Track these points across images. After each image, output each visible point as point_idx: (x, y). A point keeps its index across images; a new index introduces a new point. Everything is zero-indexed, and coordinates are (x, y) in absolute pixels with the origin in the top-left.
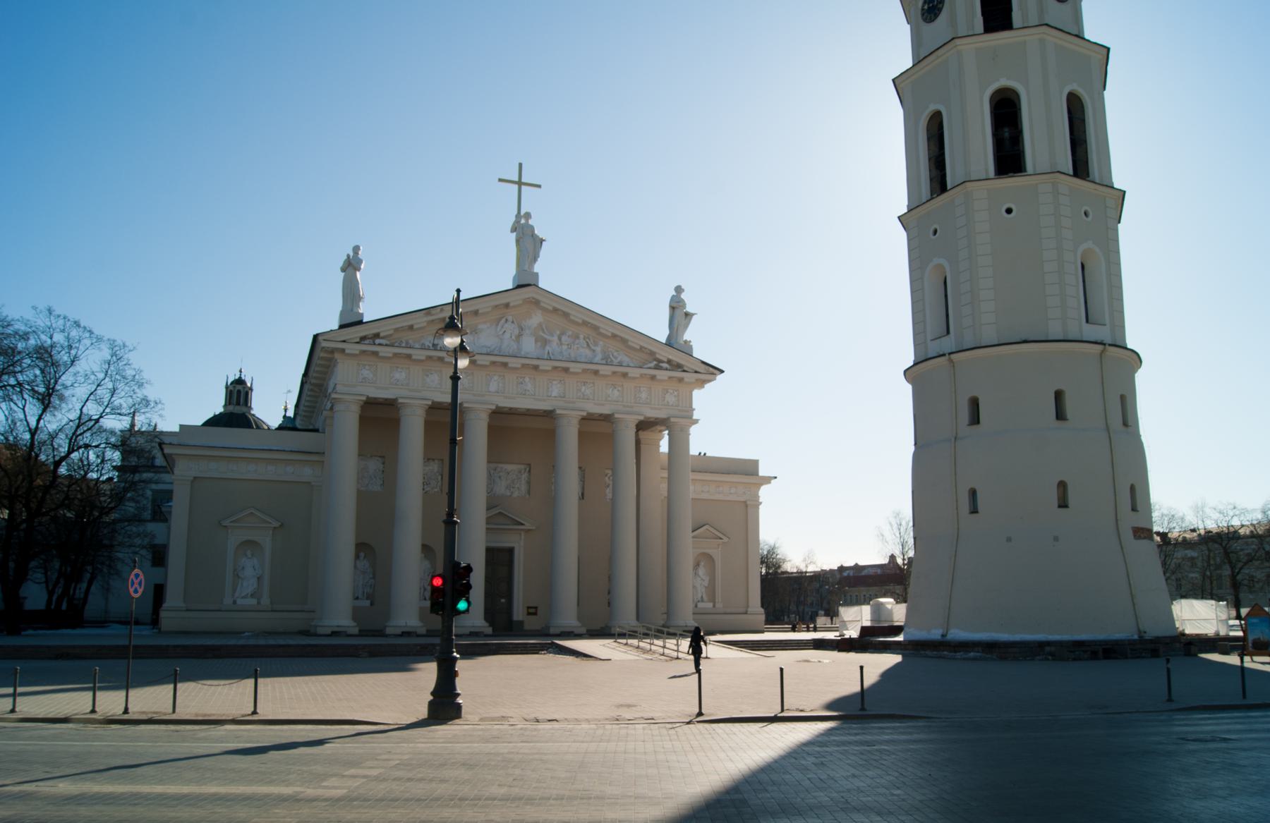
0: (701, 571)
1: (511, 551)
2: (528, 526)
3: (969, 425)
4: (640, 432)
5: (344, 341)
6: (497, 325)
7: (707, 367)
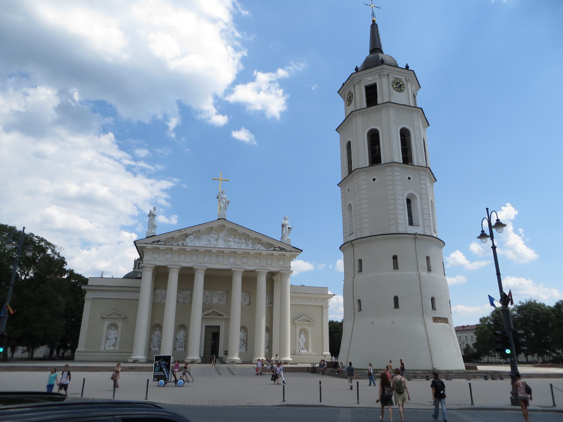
0: (302, 336)
2: (225, 317)
3: (358, 272)
4: (274, 277)
5: (146, 243)
7: (295, 249)
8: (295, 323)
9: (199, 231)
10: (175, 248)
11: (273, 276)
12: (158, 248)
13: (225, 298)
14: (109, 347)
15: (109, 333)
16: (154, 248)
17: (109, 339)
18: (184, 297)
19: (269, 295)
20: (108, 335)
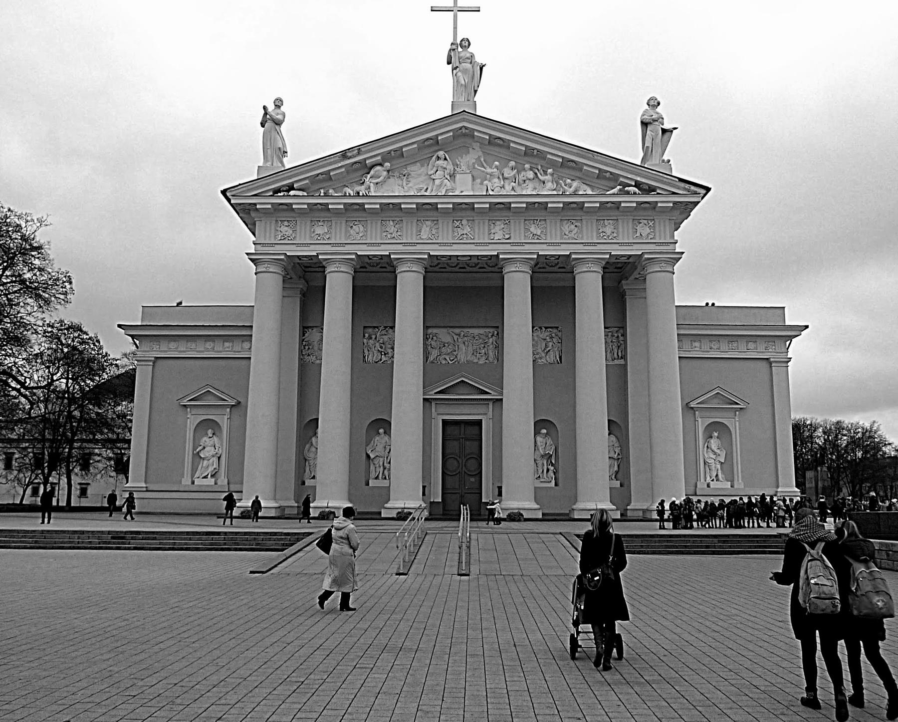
1: (479, 423)
8: (692, 408)
9: (400, 153)
10: (336, 203)
11: (621, 281)
13: (491, 346)
17: (204, 459)
18: (381, 347)
19: (613, 336)
20: (200, 448)
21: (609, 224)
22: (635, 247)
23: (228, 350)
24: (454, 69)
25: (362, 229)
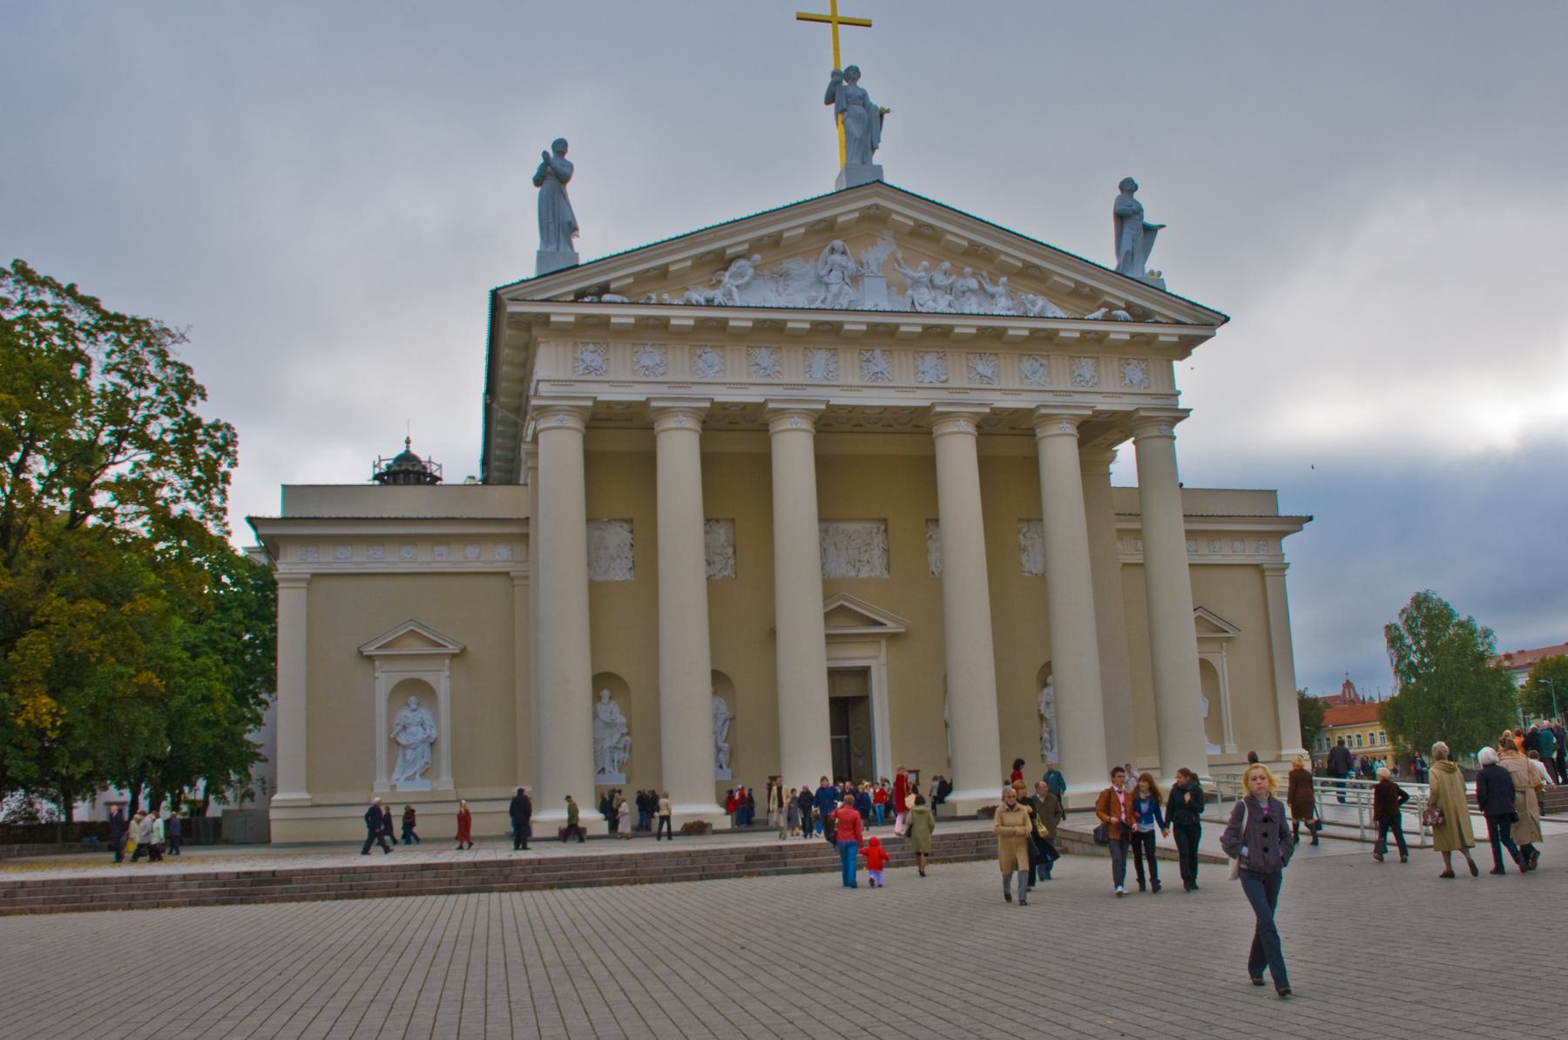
1: (864, 673)
2: (891, 627)
5: (547, 300)
6: (817, 260)
9: (776, 241)
10: (682, 318)
12: (603, 323)
14: (408, 779)
15: (397, 725)
16: (583, 321)
21: (1087, 363)
22: (1126, 399)
23: (438, 559)
24: (839, 111)
25: (717, 359)
